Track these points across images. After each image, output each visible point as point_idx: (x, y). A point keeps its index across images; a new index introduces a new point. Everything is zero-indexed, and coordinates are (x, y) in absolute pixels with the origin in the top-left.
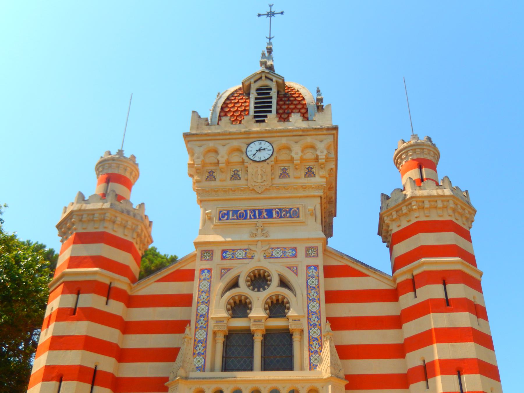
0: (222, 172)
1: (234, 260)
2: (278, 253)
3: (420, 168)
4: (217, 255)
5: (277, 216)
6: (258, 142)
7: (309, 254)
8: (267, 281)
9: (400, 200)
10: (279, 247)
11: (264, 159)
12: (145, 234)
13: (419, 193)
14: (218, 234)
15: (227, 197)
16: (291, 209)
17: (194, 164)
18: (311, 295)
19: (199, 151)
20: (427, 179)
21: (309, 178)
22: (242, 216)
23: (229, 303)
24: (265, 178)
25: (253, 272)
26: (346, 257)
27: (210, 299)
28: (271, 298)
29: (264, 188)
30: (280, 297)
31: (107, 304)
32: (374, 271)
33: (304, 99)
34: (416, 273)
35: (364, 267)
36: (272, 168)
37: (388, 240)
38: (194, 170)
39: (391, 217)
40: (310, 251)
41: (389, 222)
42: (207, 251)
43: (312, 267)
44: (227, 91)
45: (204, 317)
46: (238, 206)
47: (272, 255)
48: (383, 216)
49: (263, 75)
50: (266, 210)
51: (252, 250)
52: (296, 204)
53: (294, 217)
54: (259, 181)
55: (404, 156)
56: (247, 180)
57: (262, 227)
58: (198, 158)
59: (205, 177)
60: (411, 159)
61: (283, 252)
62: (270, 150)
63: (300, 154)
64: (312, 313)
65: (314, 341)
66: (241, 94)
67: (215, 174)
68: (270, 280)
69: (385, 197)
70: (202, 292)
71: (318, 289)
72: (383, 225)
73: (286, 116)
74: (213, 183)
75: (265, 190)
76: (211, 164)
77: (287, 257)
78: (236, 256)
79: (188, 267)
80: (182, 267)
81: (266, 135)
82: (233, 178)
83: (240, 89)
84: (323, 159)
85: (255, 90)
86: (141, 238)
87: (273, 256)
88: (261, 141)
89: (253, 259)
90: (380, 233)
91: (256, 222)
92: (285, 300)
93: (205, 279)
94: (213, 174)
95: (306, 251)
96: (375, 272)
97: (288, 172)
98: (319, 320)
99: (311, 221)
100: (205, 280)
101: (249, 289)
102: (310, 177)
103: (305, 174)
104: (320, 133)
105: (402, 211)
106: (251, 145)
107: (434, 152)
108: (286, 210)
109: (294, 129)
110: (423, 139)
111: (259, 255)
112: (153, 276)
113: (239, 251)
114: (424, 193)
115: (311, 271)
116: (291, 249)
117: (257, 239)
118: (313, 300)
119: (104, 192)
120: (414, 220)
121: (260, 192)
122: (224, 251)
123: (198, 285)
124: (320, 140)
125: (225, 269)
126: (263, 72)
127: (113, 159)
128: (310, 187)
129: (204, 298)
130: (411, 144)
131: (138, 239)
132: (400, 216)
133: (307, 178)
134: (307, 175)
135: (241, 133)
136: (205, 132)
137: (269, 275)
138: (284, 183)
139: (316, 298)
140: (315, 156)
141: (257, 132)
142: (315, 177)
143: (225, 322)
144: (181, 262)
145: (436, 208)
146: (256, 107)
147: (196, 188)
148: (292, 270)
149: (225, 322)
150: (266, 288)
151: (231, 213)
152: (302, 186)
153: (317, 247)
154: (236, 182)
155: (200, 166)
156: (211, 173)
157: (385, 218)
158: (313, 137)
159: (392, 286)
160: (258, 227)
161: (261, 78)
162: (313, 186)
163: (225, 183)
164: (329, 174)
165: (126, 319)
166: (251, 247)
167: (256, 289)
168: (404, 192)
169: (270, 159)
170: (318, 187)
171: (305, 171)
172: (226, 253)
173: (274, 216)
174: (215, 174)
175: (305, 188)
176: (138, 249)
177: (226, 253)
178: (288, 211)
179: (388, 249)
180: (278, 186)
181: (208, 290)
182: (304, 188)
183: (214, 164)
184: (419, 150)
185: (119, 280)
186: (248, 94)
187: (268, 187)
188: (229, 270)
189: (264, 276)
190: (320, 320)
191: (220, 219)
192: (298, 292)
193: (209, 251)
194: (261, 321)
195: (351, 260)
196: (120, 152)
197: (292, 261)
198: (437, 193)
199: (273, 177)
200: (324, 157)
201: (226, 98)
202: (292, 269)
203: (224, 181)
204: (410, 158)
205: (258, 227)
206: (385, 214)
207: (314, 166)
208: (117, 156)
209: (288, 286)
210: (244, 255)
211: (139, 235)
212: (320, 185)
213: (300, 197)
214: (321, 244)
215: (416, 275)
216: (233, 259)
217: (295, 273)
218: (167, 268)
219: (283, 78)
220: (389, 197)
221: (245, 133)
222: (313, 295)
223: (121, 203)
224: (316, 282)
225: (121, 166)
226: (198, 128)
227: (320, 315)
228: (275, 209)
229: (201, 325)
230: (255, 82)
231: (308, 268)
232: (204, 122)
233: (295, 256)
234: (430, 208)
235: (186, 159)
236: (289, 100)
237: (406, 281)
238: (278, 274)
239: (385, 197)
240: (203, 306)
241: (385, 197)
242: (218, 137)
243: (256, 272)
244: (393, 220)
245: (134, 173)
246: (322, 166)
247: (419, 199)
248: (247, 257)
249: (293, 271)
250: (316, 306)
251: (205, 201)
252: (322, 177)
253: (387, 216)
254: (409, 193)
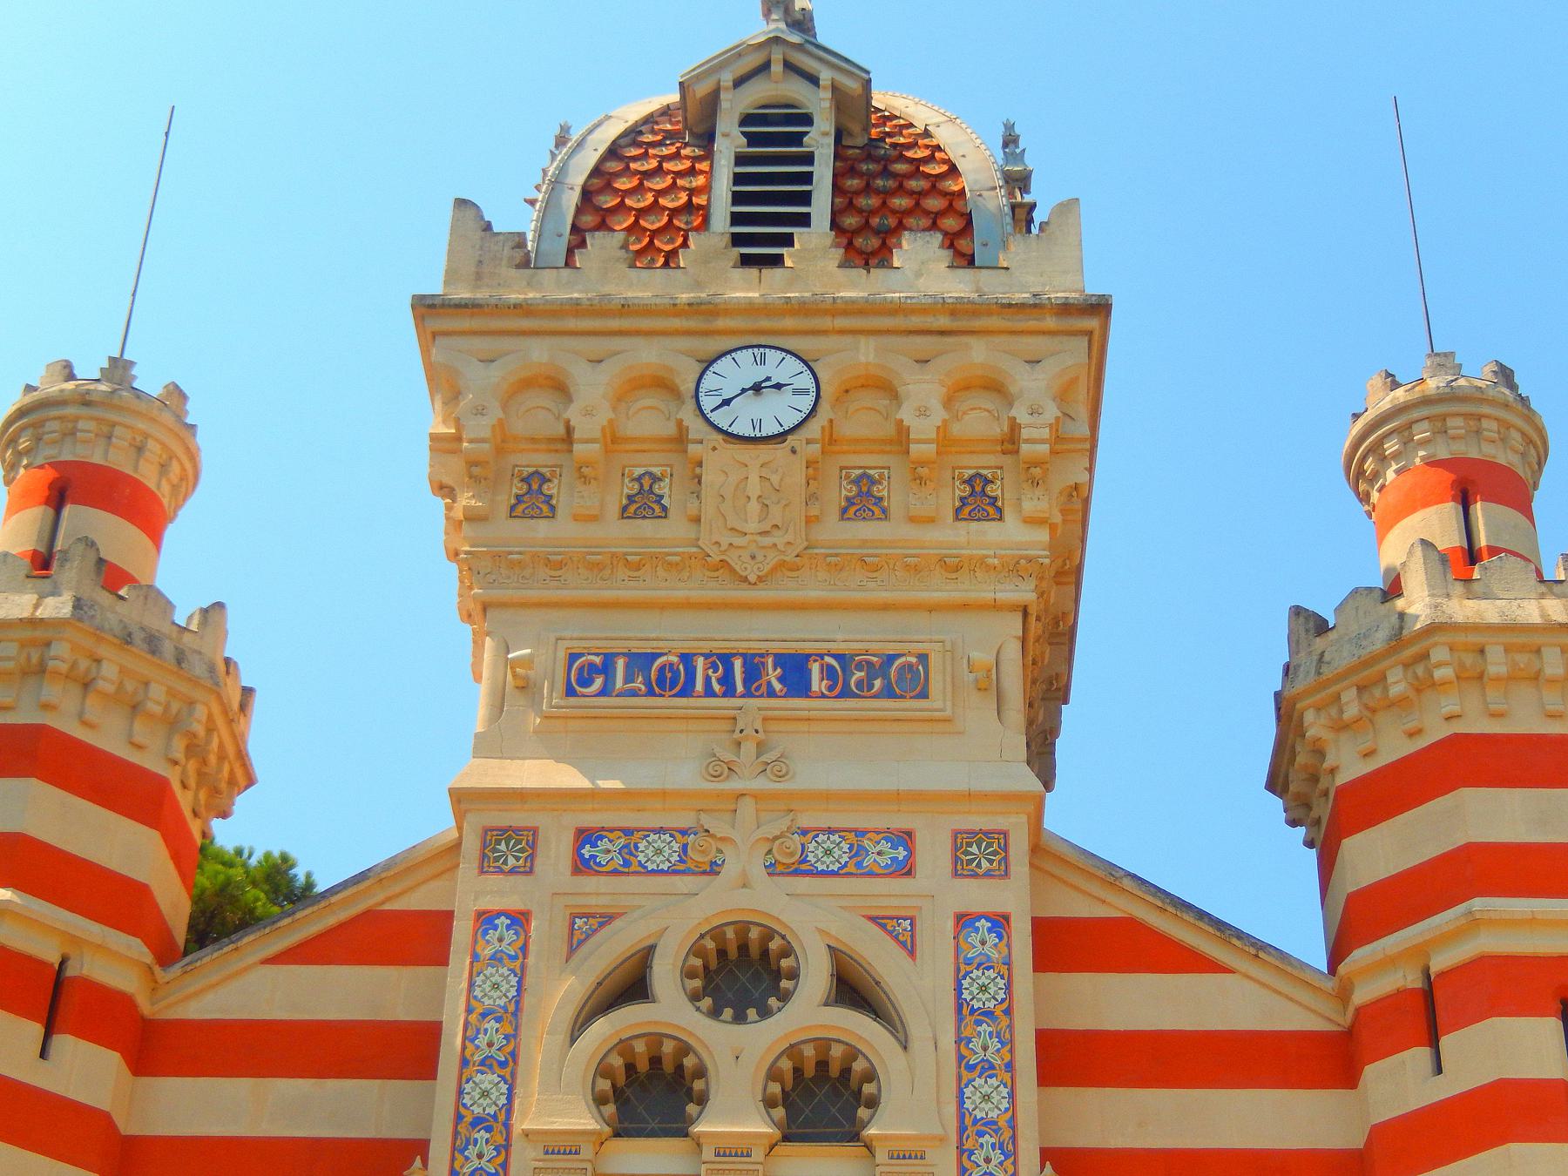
0: (585, 479)
1: (632, 878)
2: (828, 852)
3: (1466, 503)
4: (556, 851)
5: (830, 688)
6: (750, 350)
7: (970, 862)
8: (777, 975)
9: (1379, 641)
10: (834, 825)
11: (777, 429)
12: (221, 746)
13: (1463, 609)
14: (558, 760)
15: (608, 595)
16: (891, 659)
17: (458, 439)
18: (976, 1044)
19: (482, 379)
20: (1494, 551)
21: (974, 525)
23: (603, 1071)
24: (776, 515)
25: (717, 933)
26: (1127, 883)
27: (517, 1046)
28: (792, 1051)
29: (773, 558)
30: (836, 1052)
31: (43, 1054)
32: (1253, 951)
33: (953, 171)
34: (1439, 963)
35: (1211, 930)
36: (811, 471)
37: (1314, 814)
38: (456, 464)
39: (1334, 712)
40: (974, 849)
41: (1326, 735)
42: (506, 833)
43: (983, 920)
44: (608, 117)
45: (489, 1129)
46: (653, 635)
47: (805, 861)
48: (1298, 706)
49: (777, 56)
50: (780, 660)
51: (713, 836)
52: (916, 638)
53: (905, 697)
54: (752, 526)
55: (1391, 446)
56: (697, 520)
57: (761, 736)
58: (480, 411)
59: (505, 499)
60: (1423, 458)
61: (851, 849)
62: (805, 392)
63: (938, 415)
64: (978, 1127)
66: (669, 135)
67: (550, 489)
68: (794, 975)
69: (1308, 624)
70: (484, 1015)
71: (1005, 1022)
72: (1293, 747)
73: (873, 243)
74: (541, 529)
75: (774, 569)
76: (533, 440)
77: (871, 874)
78: (641, 857)
79: (419, 900)
80: (388, 899)
81: (789, 323)
82: (632, 508)
83: (666, 112)
84: (1042, 441)
85: (736, 121)
86: (204, 762)
87: (804, 867)
88: (762, 350)
89: (718, 873)
90: (1276, 783)
91: (733, 709)
92: (858, 1066)
93: (496, 959)
94: (540, 486)
95: (956, 848)
96: (1257, 956)
97: (879, 491)
98: (1007, 1157)
99: (978, 716)
100: (500, 960)
101: (698, 1009)
102: (979, 520)
103: (957, 504)
104: (1032, 324)
105: (1386, 689)
106: (716, 367)
107: (1523, 434)
108: (869, 663)
109: (914, 301)
110: (1477, 373)
111: (743, 861)
112: (258, 934)
113: (652, 837)
114: (1488, 611)
115: (974, 939)
117: (735, 784)
118: (984, 1070)
119: (42, 549)
120: (1437, 732)
121: (753, 578)
122: (586, 836)
123: (464, 985)
124: (1027, 360)
125: (587, 916)
126: (776, 40)
127: (85, 400)
128: (980, 565)
129: (490, 1045)
130: (1428, 393)
131: (192, 766)
132: (1374, 711)
133: (963, 524)
134: (967, 510)
135: (675, 310)
136: (514, 296)
137: (787, 952)
138: (864, 543)
139: (997, 1062)
140: (1006, 429)
141: (750, 309)
142: (1001, 519)
143: (587, 1152)
144: (383, 875)
145: (1536, 678)
146: (738, 198)
147: (468, 548)
148: (890, 933)
149: (587, 1152)
150: (775, 1010)
151: (620, 664)
152: (942, 560)
153: (1005, 834)
154: (646, 528)
155: (486, 446)
156: (535, 482)
157: (1309, 716)
158: (997, 340)
159: (1330, 1020)
160: (741, 731)
161: (765, 67)
162: (990, 561)
163: (593, 531)
164: (1063, 512)
165: (128, 1126)
166: (707, 821)
167: (728, 1013)
168: (1400, 603)
170: (1015, 568)
171: (958, 493)
172: (594, 845)
173: (815, 687)
174: (550, 489)
175: (957, 569)
176: (188, 814)
177: (594, 845)
178: (877, 666)
179: (1312, 854)
180: (836, 555)
181: (512, 1008)
182: (952, 566)
183: (551, 440)
184: (1459, 422)
185: (99, 947)
186: (707, 139)
187: (789, 558)
188: (608, 919)
189: (765, 953)
190: (1012, 1159)
191: (570, 692)
192: (918, 1030)
193: (516, 830)
194: (749, 1155)
195: (1150, 898)
196: (119, 368)
197: (890, 893)
198: (1543, 614)
199: (814, 511)
200: (1045, 434)
201: (602, 149)
202: (889, 928)
203: (593, 518)
204: (1421, 453)
205: (741, 731)
206: (1310, 700)
207: (999, 471)
208: (103, 387)
209: (870, 1005)
210: (675, 857)
211: (191, 750)
212: (1022, 557)
213: (932, 608)
214: (1024, 818)
215: (1442, 975)
216: (626, 870)
217: (903, 945)
218: (323, 904)
219: (868, 72)
220: (1326, 622)
221: (694, 308)
222: (985, 1048)
223: (122, 598)
224: (997, 988)
225: (118, 431)
226: (479, 276)
227: (1014, 1138)
228: (821, 656)
229: (476, 1163)
230: (739, 82)
231: (965, 926)
232: (507, 251)
233: (906, 869)
234: (1512, 678)
235: (427, 418)
236: (886, 173)
237: (1398, 998)
238: (829, 946)
239: (1308, 624)
240: (487, 1080)
241: (1311, 624)
242: (572, 324)
243: (730, 934)
244: (1341, 727)
245: (175, 468)
246: (1037, 471)
247: (1460, 638)
248: (690, 864)
249: (896, 938)
250: (995, 1098)
251: (503, 605)
252: (1033, 521)
253: (1318, 710)
254: (1418, 603)
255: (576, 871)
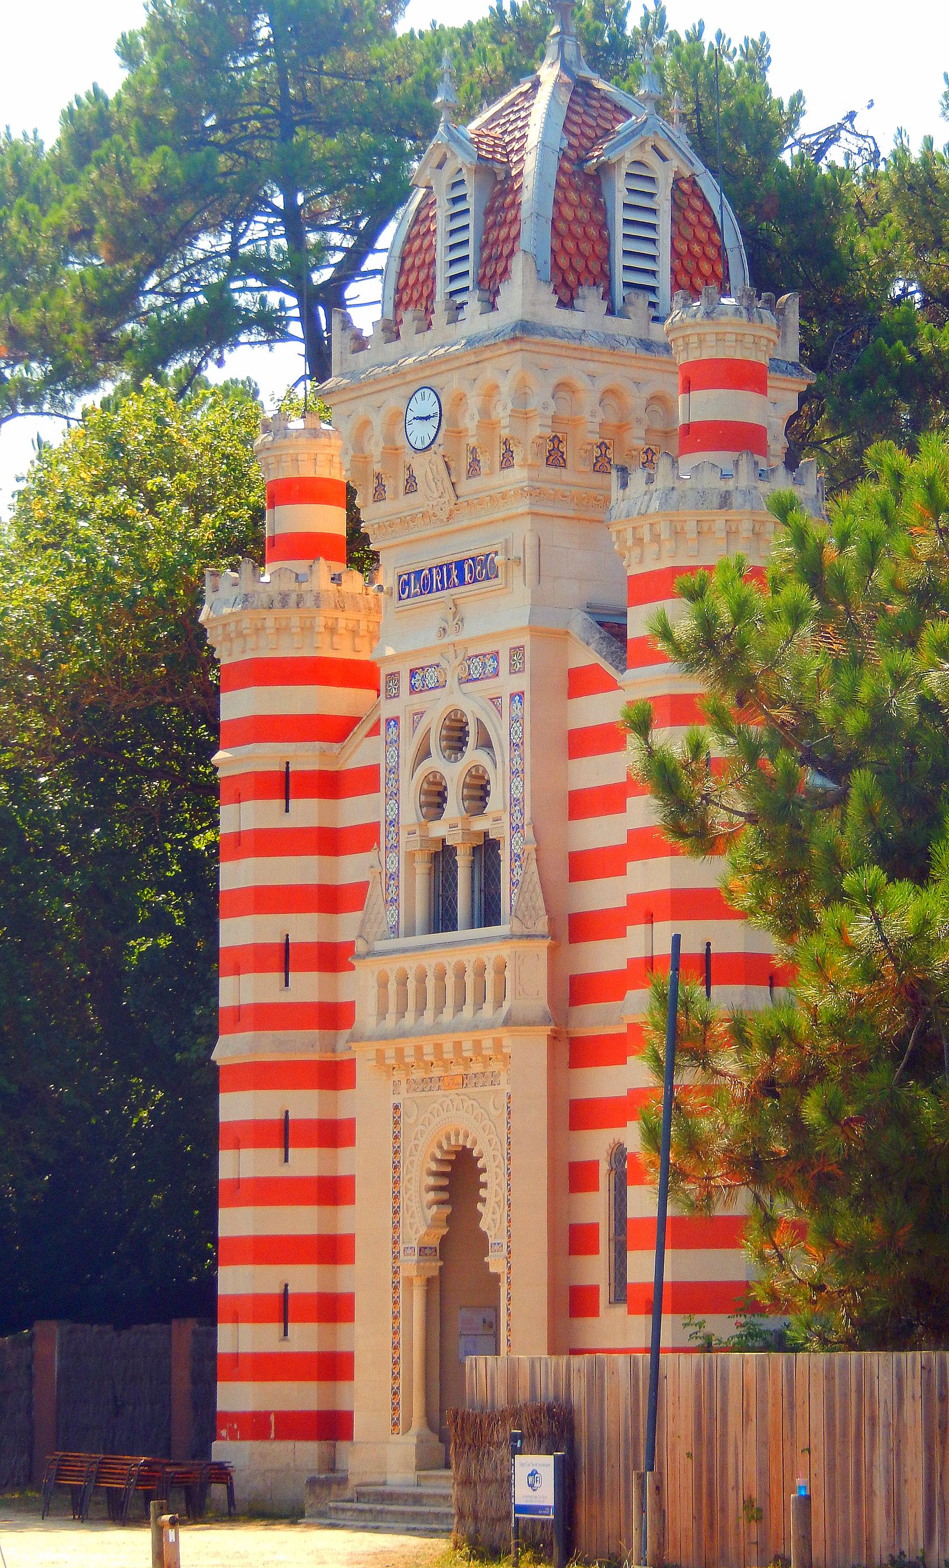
22: (427, 588)
54: (436, 495)
65: (516, 861)
77: (488, 678)
87: (470, 677)
116: (492, 657)
117: (446, 640)
169: (440, 439)
191: (400, 599)
233: (496, 674)
255: (411, 693)
